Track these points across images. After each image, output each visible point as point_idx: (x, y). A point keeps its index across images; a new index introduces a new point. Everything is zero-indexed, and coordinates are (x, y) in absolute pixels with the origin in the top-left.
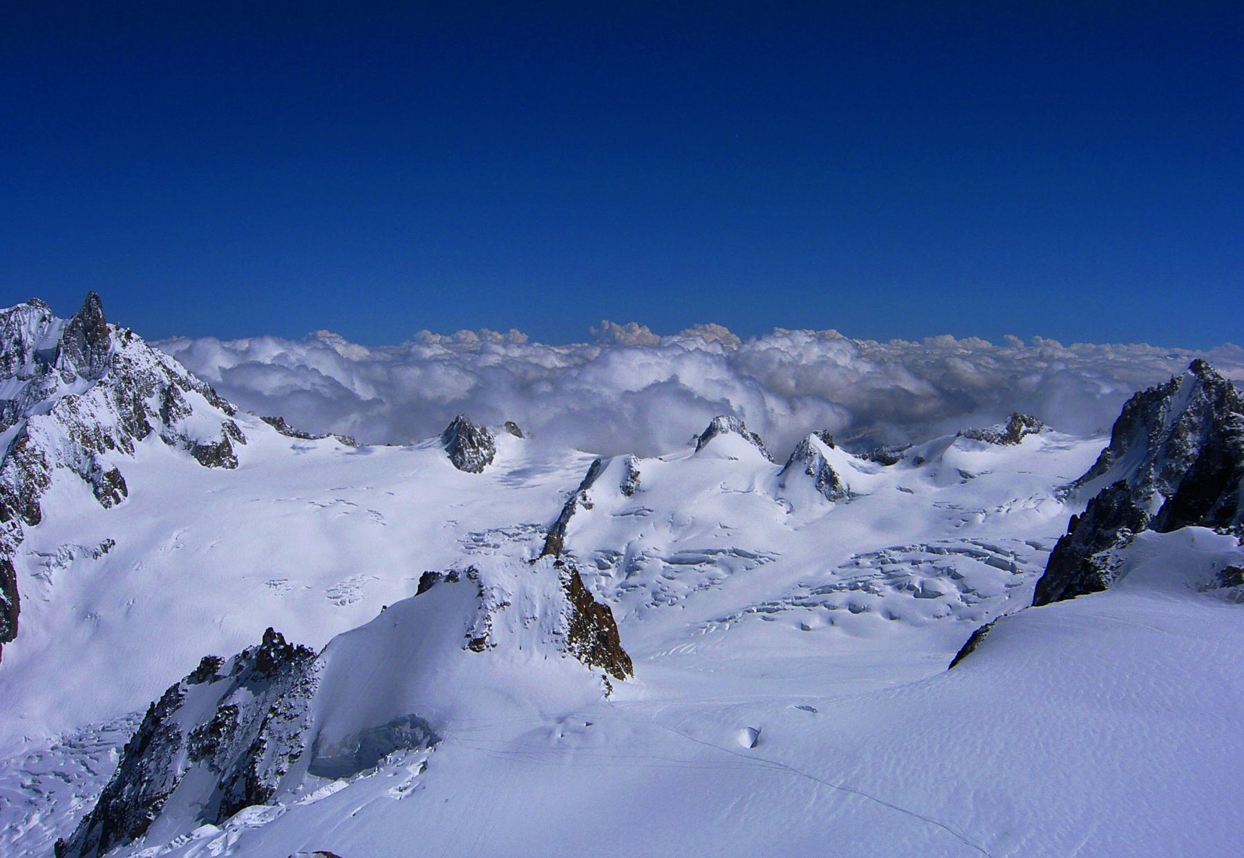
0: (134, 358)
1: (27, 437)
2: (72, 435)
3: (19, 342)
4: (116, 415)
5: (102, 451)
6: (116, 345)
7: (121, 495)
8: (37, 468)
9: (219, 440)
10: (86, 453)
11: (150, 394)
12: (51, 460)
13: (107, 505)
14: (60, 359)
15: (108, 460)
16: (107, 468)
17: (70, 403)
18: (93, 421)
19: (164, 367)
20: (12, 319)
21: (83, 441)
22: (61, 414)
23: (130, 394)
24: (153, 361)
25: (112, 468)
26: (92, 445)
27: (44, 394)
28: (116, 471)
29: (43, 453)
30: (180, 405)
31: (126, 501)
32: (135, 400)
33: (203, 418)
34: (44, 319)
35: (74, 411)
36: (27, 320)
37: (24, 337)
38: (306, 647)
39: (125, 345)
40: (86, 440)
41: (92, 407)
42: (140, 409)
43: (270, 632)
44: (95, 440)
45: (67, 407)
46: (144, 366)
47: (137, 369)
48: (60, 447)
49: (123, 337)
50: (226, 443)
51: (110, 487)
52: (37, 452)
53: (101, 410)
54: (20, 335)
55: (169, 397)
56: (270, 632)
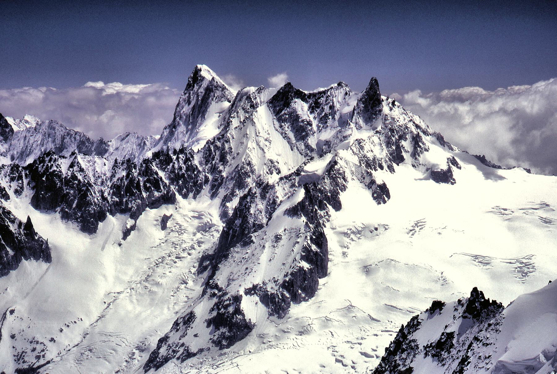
0: (396, 117)
1: (336, 163)
2: (360, 162)
3: (332, 107)
4: (385, 151)
5: (376, 170)
6: (386, 109)
7: (386, 199)
8: (340, 181)
9: (444, 167)
10: (368, 173)
11: (406, 139)
12: (348, 175)
13: (379, 203)
14: (354, 117)
15: (380, 176)
16: (379, 182)
17: (360, 143)
18: (372, 154)
19: (414, 123)
20: (329, 93)
21: (366, 166)
22: (355, 150)
23: (393, 139)
24: (407, 119)
25: (382, 183)
26: (371, 169)
27: (345, 137)
28: (384, 185)
29: (344, 172)
30: (422, 146)
31: (389, 202)
32: (396, 142)
33: (437, 156)
34: (346, 94)
35: (362, 148)
36: (336, 94)
37: (335, 103)
38: (498, 302)
39: (391, 109)
40: (368, 165)
41: (372, 146)
42: (399, 148)
43: (475, 289)
44: (371, 164)
45: (357, 146)
46: (402, 122)
47: (398, 124)
48: (353, 169)
49: (390, 105)
50: (449, 170)
51: (381, 193)
52: (341, 172)
53: (377, 150)
54: (333, 103)
55: (416, 140)
56: (475, 289)
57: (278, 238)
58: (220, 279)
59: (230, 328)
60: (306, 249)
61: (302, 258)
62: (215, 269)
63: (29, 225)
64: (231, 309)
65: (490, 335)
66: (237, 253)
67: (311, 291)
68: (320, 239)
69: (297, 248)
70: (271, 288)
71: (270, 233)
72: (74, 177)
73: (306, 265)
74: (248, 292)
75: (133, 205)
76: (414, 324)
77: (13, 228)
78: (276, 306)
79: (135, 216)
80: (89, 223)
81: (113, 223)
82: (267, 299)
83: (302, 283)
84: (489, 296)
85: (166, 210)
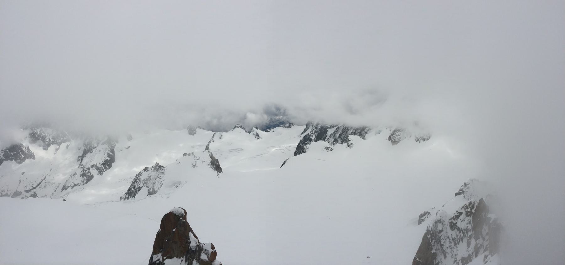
57: (100, 151)
58: (84, 163)
59: (87, 178)
60: (108, 154)
61: (108, 156)
62: (82, 160)
63: (28, 148)
64: (87, 172)
65: (162, 176)
66: (89, 155)
67: (110, 166)
68: (112, 151)
69: (106, 154)
70: (99, 165)
71: (98, 149)
72: (41, 134)
73: (108, 159)
74: (92, 166)
75: (58, 142)
76: (140, 174)
77: (24, 149)
78: (100, 172)
79: (59, 145)
80: (46, 147)
81: (52, 147)
82: (97, 168)
83: (108, 164)
84: (161, 165)
85: (68, 143)
